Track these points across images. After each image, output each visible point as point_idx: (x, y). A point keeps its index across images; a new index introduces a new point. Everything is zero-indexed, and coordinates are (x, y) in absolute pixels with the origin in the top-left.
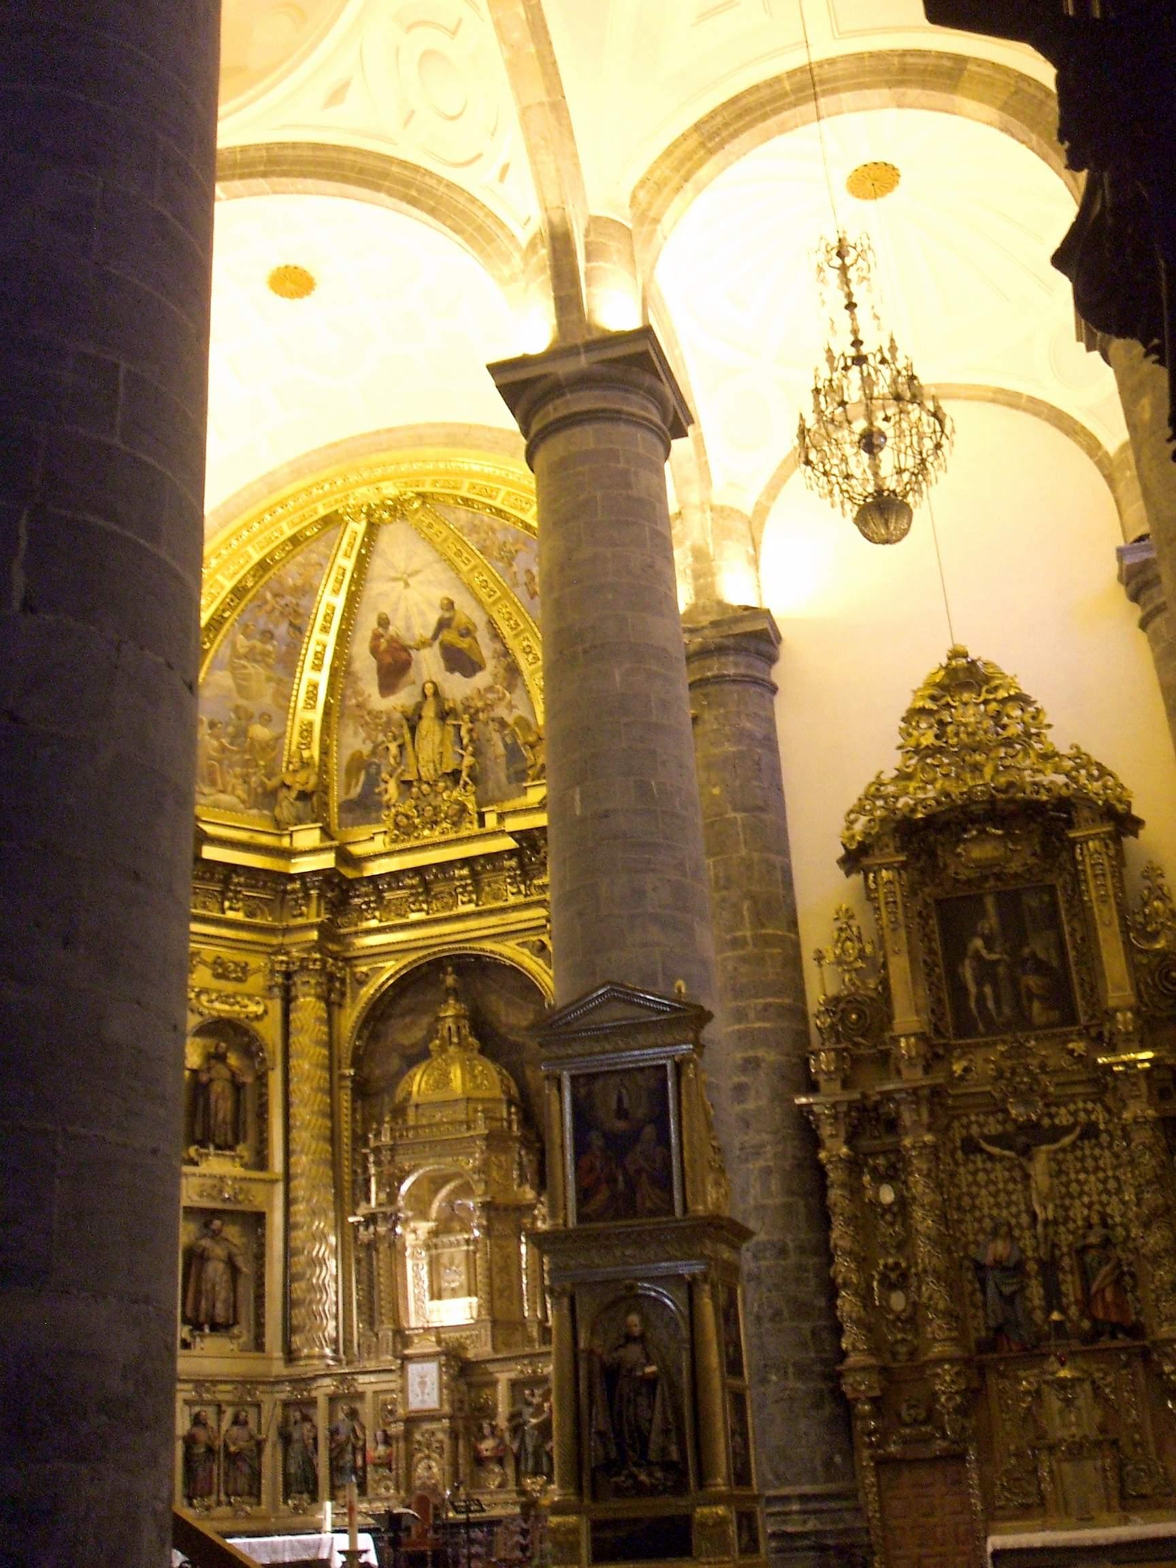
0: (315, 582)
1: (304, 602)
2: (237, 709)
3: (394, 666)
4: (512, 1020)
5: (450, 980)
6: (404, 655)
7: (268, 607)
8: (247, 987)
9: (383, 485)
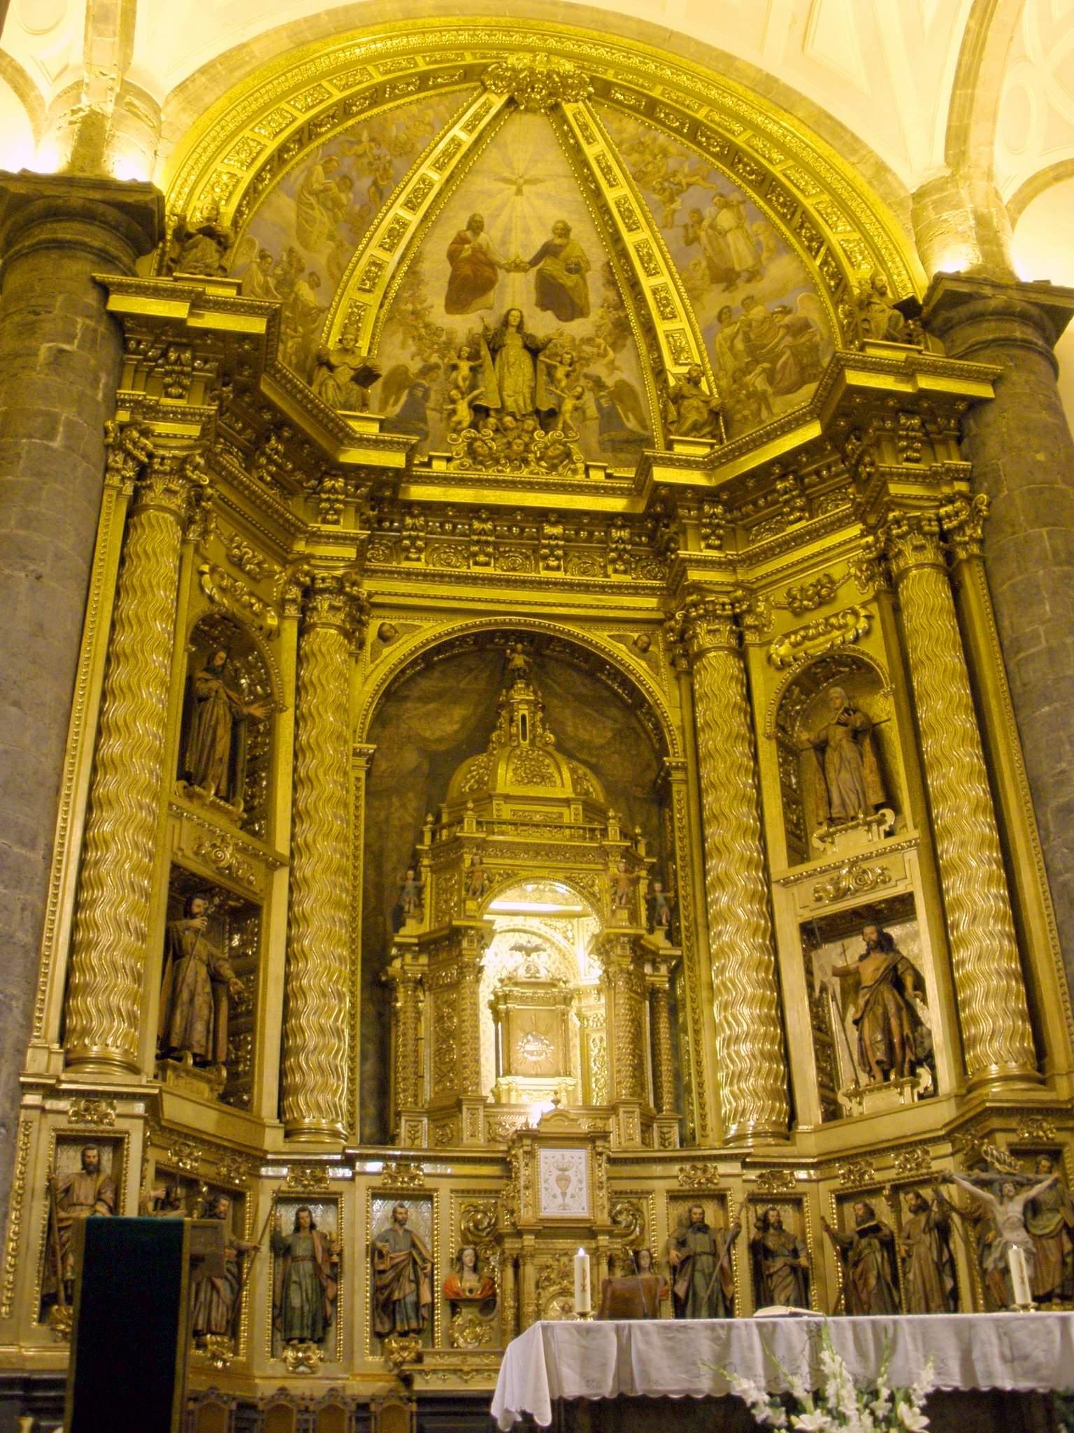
0: (419, 146)
1: (397, 162)
2: (291, 251)
3: (471, 279)
4: (584, 735)
5: (519, 661)
6: (488, 272)
7: (359, 149)
8: (260, 589)
9: (554, 59)
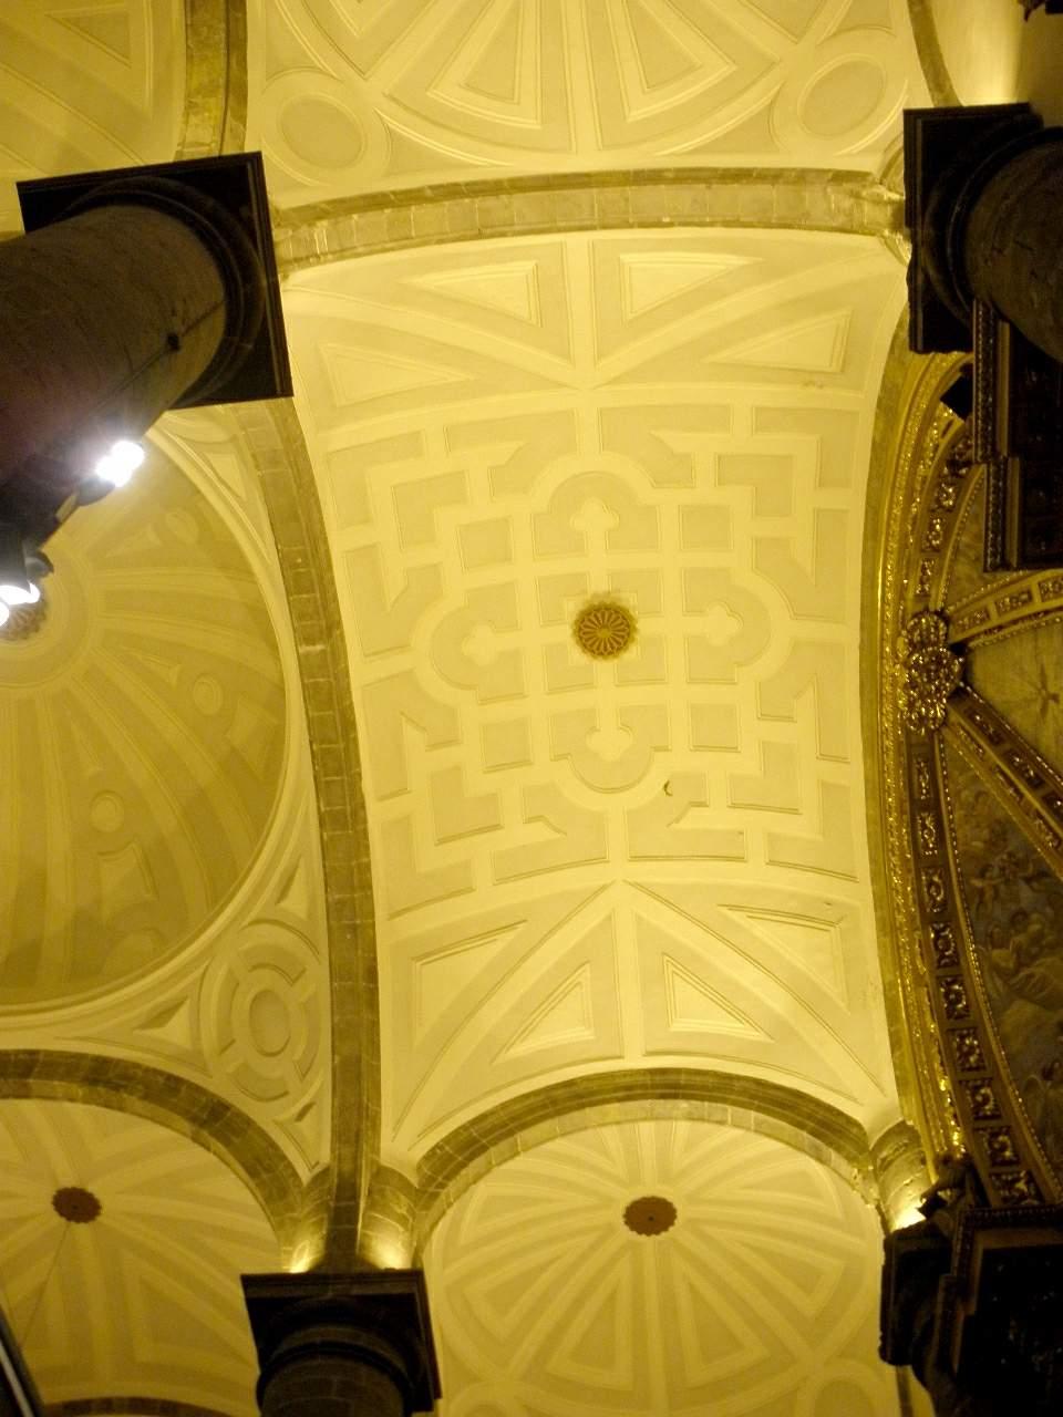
0: (999, 814)
7: (989, 894)
